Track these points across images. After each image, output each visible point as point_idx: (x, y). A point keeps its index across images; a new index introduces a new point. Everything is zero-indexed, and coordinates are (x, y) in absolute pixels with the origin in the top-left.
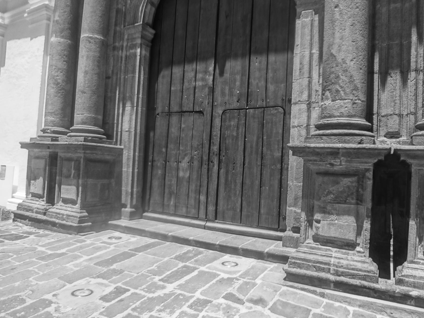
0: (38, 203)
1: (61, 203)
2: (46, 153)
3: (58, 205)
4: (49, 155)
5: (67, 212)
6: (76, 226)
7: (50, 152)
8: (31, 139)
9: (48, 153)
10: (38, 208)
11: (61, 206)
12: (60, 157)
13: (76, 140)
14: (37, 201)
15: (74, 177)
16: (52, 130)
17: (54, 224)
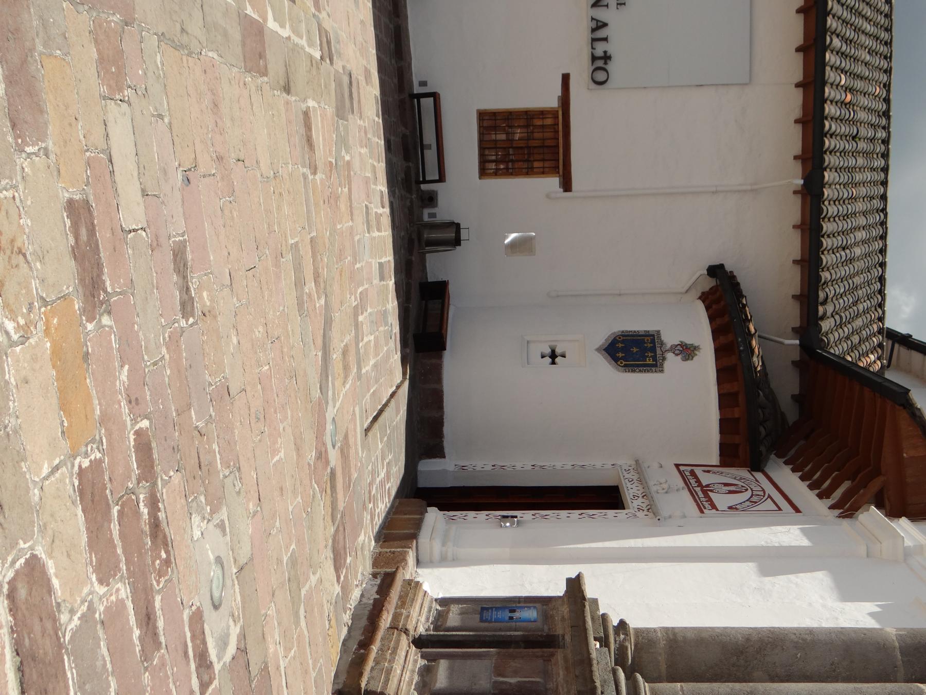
0: (423, 619)
1: (421, 662)
2: (561, 629)
3: (416, 654)
4: (554, 636)
5: (399, 672)
6: (360, 685)
7: (563, 636)
8: (595, 602)
9: (559, 631)
10: (408, 616)
11: (416, 661)
12: (552, 655)
13: (604, 683)
14: (428, 619)
15: (495, 682)
16: (627, 644)
17: (365, 644)
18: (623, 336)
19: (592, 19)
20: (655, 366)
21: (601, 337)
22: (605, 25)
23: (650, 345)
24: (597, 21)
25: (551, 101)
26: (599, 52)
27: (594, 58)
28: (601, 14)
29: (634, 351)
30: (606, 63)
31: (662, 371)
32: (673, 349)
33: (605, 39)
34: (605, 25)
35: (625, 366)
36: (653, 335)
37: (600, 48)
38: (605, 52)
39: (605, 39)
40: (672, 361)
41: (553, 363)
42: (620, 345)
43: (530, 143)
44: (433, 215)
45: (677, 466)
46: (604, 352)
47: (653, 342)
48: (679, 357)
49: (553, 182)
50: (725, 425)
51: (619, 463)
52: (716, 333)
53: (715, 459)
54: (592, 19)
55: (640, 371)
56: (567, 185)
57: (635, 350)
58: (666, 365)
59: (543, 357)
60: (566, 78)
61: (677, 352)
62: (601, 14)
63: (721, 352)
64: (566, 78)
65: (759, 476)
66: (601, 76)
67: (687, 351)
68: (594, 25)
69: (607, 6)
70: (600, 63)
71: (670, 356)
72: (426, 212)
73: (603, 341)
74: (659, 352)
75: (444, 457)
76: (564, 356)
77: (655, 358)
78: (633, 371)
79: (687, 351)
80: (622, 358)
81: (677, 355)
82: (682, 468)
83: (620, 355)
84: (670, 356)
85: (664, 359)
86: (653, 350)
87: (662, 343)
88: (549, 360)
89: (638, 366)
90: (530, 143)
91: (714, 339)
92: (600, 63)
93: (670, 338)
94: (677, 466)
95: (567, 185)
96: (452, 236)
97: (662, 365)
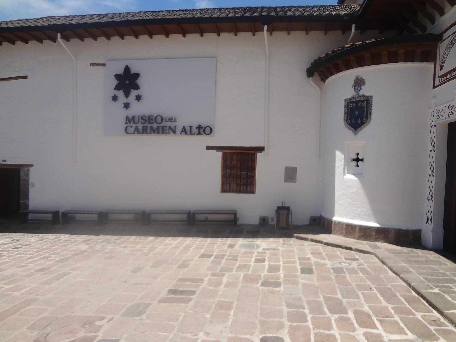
18: (347, 119)
19: (181, 134)
20: (367, 101)
21: (348, 132)
22: (184, 128)
23: (354, 104)
24: (182, 131)
25: (219, 155)
26: (196, 131)
27: (199, 133)
28: (179, 129)
29: (358, 114)
30: (202, 128)
31: (371, 97)
32: (357, 91)
33: (191, 127)
34: (184, 128)
35: (367, 118)
36: (348, 103)
37: (195, 130)
38: (197, 128)
39: (191, 127)
40: (365, 91)
41: (362, 160)
42: (353, 121)
43: (239, 167)
44: (272, 219)
45: (434, 87)
46: (357, 131)
47: (352, 103)
48: (363, 87)
49: (259, 156)
50: (409, 58)
51: (430, 122)
52: (348, 67)
53: (431, 65)
54: (181, 134)
55: (371, 109)
56: (261, 149)
57: (357, 113)
58: (367, 94)
59: (358, 166)
60: (209, 148)
61: (359, 89)
62: (179, 129)
63: (361, 63)
64: (209, 148)
65: (446, 35)
66: (208, 130)
67: (359, 83)
68: (183, 133)
69: (175, 126)
70: (202, 130)
71: (361, 93)
72: (270, 222)
73: (350, 131)
74: (358, 99)
75: (421, 230)
76: (358, 154)
77: (362, 101)
78: (370, 113)
79: (359, 83)
80: (362, 120)
81: (361, 89)
82: (437, 83)
83: (359, 121)
84: (361, 93)
85: (363, 96)
86: (357, 102)
87: (353, 97)
88: (360, 163)
89: (367, 111)
90: (239, 167)
91: (352, 67)
92: (202, 130)
93: (350, 93)
94: (434, 87)
95: (261, 149)
96: (284, 211)
97: (367, 97)
